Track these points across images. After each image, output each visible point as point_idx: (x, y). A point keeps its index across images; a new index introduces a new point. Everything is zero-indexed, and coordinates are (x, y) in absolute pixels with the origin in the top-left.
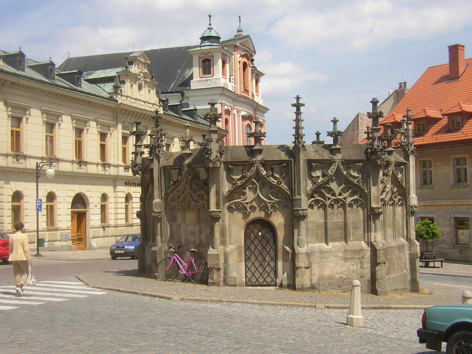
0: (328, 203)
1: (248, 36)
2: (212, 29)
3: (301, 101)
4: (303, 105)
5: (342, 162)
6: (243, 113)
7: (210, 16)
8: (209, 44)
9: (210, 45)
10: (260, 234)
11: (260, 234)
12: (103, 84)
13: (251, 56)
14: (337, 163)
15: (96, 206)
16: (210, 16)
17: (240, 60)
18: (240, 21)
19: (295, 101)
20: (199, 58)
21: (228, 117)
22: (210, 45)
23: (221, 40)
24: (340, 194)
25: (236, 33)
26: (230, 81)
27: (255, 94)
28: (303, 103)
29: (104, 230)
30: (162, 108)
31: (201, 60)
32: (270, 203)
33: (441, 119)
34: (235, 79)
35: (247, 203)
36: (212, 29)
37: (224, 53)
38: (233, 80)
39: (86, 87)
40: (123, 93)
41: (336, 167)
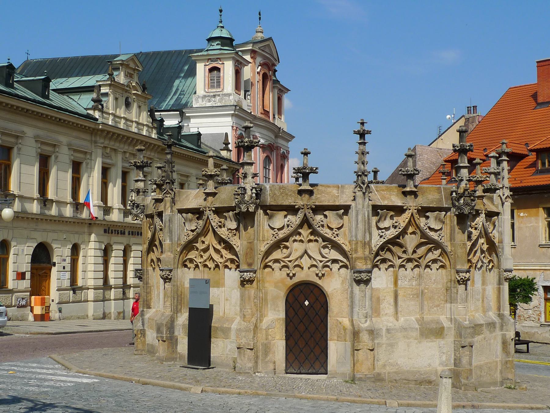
0: (398, 262)
2: (223, 27)
3: (366, 127)
4: (369, 132)
5: (418, 211)
7: (221, 11)
8: (219, 47)
9: (221, 49)
10: (307, 303)
11: (307, 303)
12: (78, 97)
13: (274, 65)
14: (411, 211)
15: (64, 260)
16: (221, 11)
18: (260, 18)
19: (358, 127)
22: (221, 49)
23: (234, 43)
24: (414, 252)
26: (245, 98)
28: (369, 130)
29: (74, 293)
30: (154, 131)
32: (321, 261)
33: (527, 156)
35: (290, 261)
36: (223, 27)
37: (238, 61)
39: (56, 99)
40: (105, 109)
41: (410, 215)
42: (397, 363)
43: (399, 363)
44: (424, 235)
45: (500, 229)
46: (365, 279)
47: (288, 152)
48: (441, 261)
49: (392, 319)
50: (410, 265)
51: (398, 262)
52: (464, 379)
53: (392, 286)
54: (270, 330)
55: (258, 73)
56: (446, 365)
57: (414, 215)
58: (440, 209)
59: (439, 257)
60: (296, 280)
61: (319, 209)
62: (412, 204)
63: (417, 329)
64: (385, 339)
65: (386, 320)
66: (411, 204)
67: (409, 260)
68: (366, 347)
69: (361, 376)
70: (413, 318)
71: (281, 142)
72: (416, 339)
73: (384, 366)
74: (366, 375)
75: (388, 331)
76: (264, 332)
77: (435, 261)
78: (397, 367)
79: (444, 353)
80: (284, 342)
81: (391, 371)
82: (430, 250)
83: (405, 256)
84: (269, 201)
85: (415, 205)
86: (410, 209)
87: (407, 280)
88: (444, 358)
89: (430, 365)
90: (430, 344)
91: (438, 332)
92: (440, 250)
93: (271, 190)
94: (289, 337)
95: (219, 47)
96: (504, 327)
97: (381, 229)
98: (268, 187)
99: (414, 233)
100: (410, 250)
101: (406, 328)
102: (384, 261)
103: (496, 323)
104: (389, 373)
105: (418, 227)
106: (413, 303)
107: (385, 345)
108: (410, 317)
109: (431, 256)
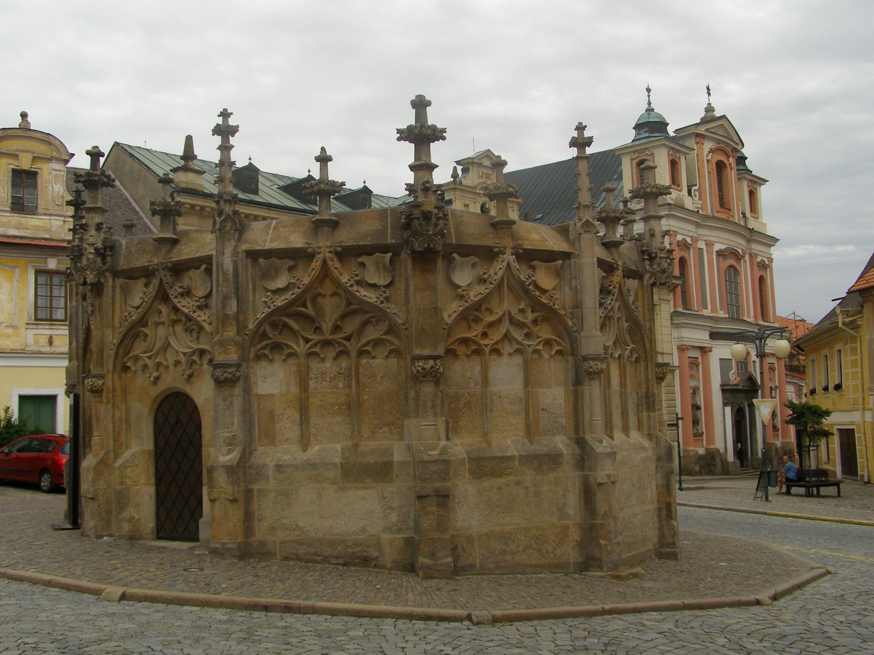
1: (724, 117)
3: (232, 122)
6: (717, 247)
8: (647, 135)
9: (648, 137)
14: (321, 255)
16: (648, 90)
17: (709, 158)
20: (632, 160)
21: (686, 255)
22: (648, 137)
24: (336, 328)
25: (702, 114)
27: (748, 214)
31: (634, 162)
34: (699, 190)
38: (697, 193)
42: (297, 526)
43: (301, 524)
44: (351, 300)
45: (574, 283)
46: (222, 378)
47: (771, 260)
48: (391, 343)
49: (295, 448)
50: (331, 353)
51: (301, 348)
52: (425, 557)
53: (295, 389)
54: (129, 470)
55: (708, 161)
56: (399, 531)
57: (330, 263)
58: (384, 249)
59: (384, 334)
60: (162, 386)
61: (178, 269)
62: (324, 244)
63: (335, 465)
64: (272, 482)
65: (282, 452)
66: (321, 244)
67: (327, 343)
68: (223, 496)
69: (217, 545)
70: (338, 447)
71: (756, 248)
72: (333, 483)
73: (272, 529)
74: (224, 544)
75: (279, 468)
76: (117, 472)
77: (377, 343)
78: (297, 533)
79: (393, 509)
80: (152, 490)
81: (288, 538)
82: (365, 324)
83: (316, 337)
84: (123, 264)
85: (328, 244)
86: (319, 253)
87: (328, 379)
88: (394, 517)
89: (364, 530)
90: (362, 493)
91: (381, 471)
92: (387, 322)
93: (127, 247)
94: (159, 481)
95: (647, 135)
96: (587, 463)
97: (268, 291)
98: (124, 242)
99: (334, 294)
100: (327, 326)
101: (315, 464)
102: (277, 347)
103: (561, 455)
104: (282, 542)
105: (338, 284)
106: (339, 419)
107: (272, 494)
108: (330, 447)
109: (372, 334)
